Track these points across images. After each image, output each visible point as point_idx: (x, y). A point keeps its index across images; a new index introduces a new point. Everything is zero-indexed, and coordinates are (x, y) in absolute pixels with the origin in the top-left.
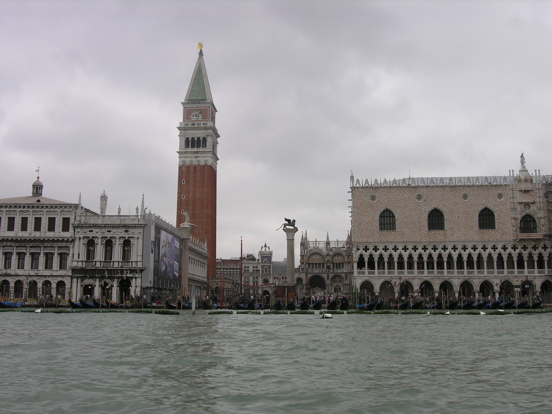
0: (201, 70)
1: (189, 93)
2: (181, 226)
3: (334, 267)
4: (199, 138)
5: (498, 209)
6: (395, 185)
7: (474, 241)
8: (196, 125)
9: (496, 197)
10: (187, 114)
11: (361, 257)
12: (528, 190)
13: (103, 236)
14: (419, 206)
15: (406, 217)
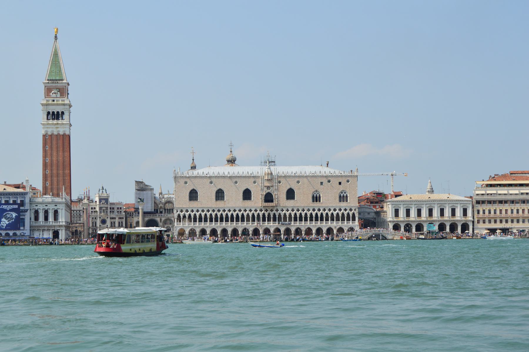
0: (57, 53)
1: (48, 73)
2: (84, 202)
3: (165, 212)
4: (58, 112)
5: (253, 189)
6: (198, 175)
7: (240, 207)
8: (55, 101)
9: (252, 182)
10: (48, 91)
11: (179, 216)
12: (269, 179)
13: (43, 208)
14: (211, 187)
15: (204, 194)
